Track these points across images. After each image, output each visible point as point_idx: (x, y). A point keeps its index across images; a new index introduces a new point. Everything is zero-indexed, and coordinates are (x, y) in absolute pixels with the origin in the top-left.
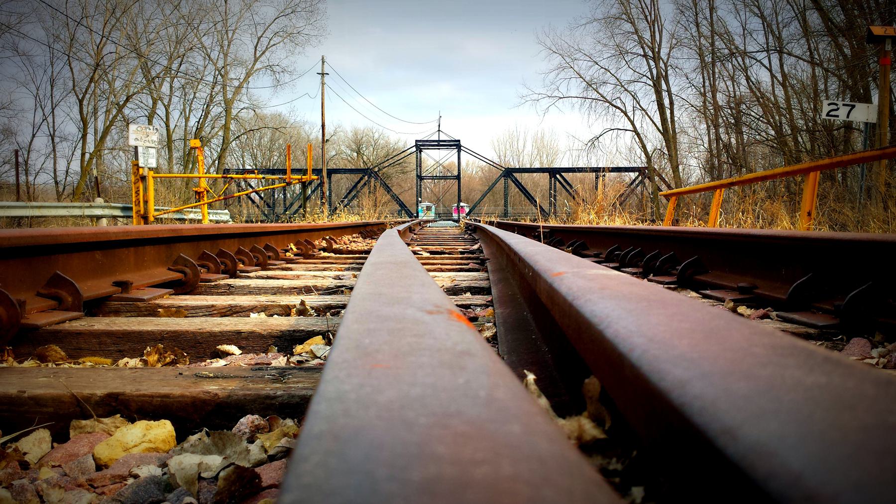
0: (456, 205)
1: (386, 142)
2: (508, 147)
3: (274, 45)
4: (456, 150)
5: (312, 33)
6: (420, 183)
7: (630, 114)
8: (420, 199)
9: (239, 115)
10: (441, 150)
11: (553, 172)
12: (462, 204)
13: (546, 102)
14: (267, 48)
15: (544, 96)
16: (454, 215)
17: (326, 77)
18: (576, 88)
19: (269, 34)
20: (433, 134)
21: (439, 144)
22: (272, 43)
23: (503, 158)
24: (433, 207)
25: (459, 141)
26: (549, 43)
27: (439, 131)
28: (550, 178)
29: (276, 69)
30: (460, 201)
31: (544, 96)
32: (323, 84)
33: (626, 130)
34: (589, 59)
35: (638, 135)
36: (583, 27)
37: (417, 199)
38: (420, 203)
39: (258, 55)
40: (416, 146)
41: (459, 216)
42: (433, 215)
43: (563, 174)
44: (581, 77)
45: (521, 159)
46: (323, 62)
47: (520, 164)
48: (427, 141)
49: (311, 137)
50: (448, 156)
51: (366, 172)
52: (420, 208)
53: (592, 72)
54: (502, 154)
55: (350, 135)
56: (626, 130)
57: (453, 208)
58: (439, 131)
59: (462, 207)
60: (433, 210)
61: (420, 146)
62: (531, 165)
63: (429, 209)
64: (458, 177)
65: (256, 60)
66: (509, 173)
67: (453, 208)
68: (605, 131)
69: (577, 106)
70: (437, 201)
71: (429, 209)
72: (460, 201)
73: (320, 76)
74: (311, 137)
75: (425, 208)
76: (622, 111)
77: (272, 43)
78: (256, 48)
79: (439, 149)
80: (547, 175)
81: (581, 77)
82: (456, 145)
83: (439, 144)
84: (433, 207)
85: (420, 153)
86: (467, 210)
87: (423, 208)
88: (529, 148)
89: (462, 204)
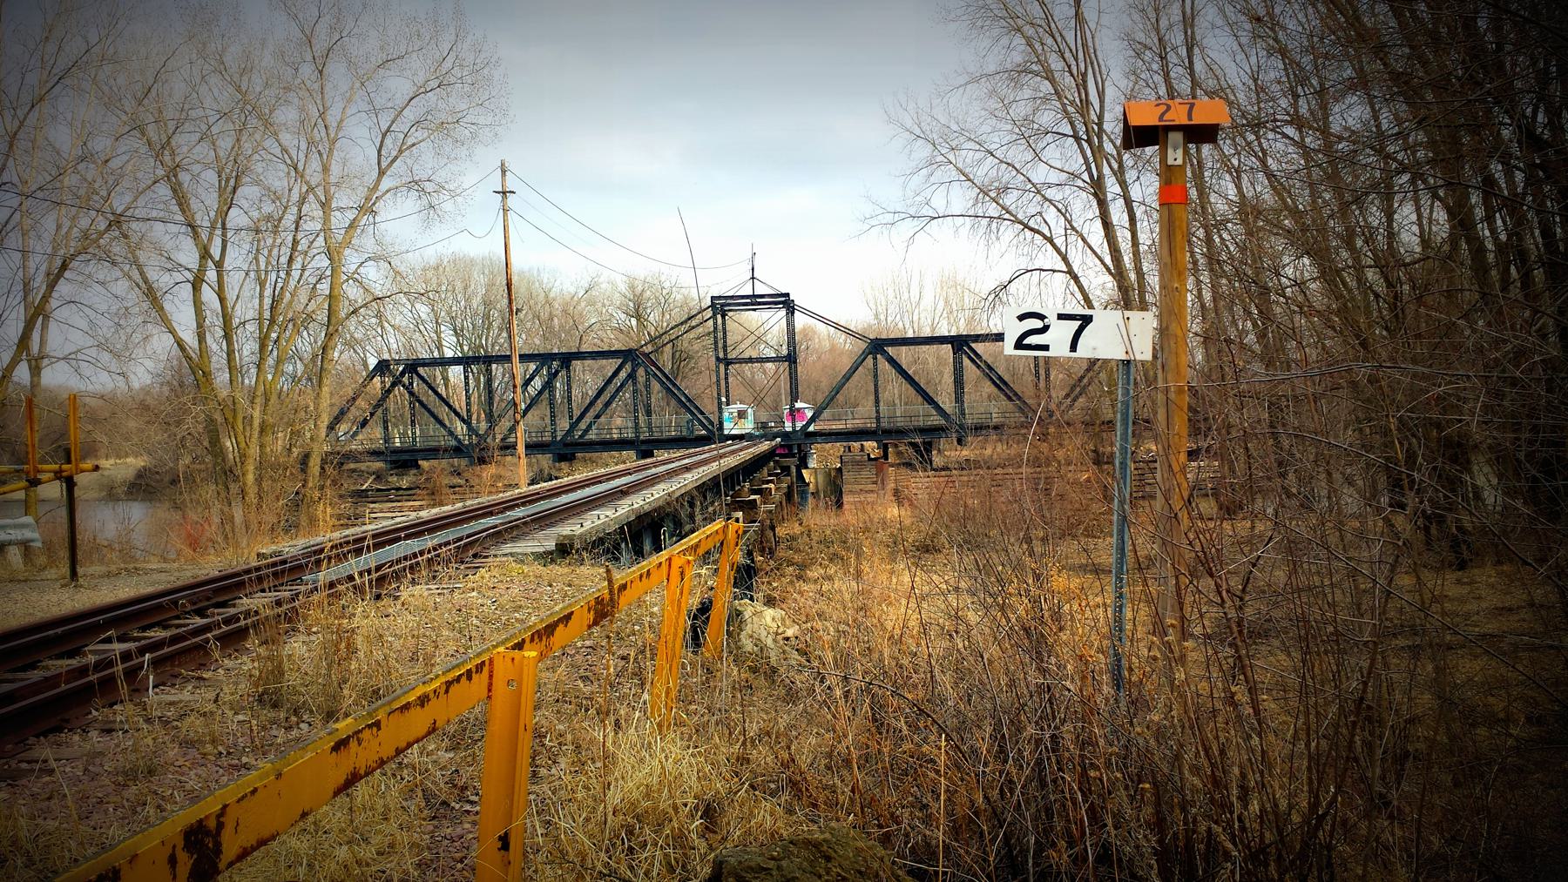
1: (686, 298)
2: (891, 297)
3: (414, 145)
4: (783, 312)
5: (481, 120)
6: (726, 369)
7: (1059, 242)
8: (724, 399)
9: (362, 270)
10: (757, 313)
11: (960, 343)
12: (798, 405)
13: (909, 226)
14: (401, 151)
15: (903, 216)
17: (510, 198)
18: (961, 198)
19: (401, 126)
20: (745, 282)
21: (754, 301)
22: (410, 141)
23: (882, 317)
24: (749, 410)
25: (788, 295)
26: (909, 123)
27: (753, 278)
29: (429, 187)
30: (794, 397)
31: (903, 216)
32: (505, 211)
33: (1054, 271)
34: (978, 147)
35: (1076, 278)
36: (961, 89)
37: (719, 399)
38: (728, 405)
39: (384, 165)
40: (713, 306)
41: (794, 426)
42: (751, 425)
43: (973, 345)
44: (969, 180)
45: (916, 318)
46: (504, 172)
47: (916, 326)
48: (732, 297)
49: (552, 295)
50: (772, 322)
51: (628, 355)
52: (726, 415)
53: (985, 170)
54: (880, 310)
55: (623, 288)
56: (1054, 271)
57: (785, 412)
58: (753, 278)
59: (799, 410)
61: (721, 306)
62: (933, 330)
63: (742, 414)
64: (791, 359)
65: (382, 173)
66: (878, 346)
67: (785, 412)
68: (1018, 274)
69: (964, 231)
70: (758, 401)
71: (742, 414)
72: (794, 397)
73: (499, 197)
74: (552, 295)
75: (736, 414)
76: (1045, 237)
77: (410, 141)
78: (379, 151)
79: (754, 310)
81: (969, 180)
82: (785, 302)
83: (754, 301)
85: (723, 317)
86: (809, 414)
87: (732, 413)
88: (927, 301)
89: (798, 405)
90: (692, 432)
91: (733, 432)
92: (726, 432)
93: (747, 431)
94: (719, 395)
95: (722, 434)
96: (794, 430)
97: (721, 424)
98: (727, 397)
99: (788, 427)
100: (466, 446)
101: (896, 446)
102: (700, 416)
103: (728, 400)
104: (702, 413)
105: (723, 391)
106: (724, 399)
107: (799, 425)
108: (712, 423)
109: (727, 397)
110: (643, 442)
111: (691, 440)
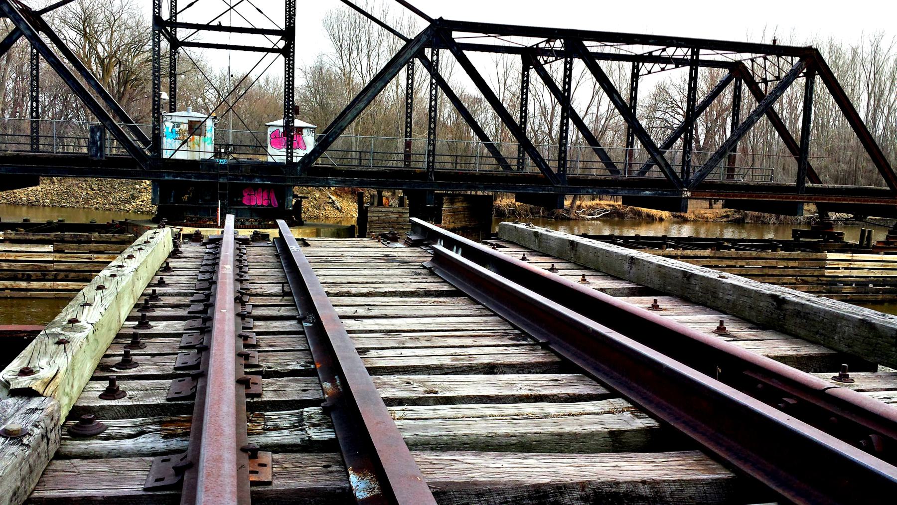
0: (281, 122)
8: (165, 96)
12: (298, 123)
16: (270, 150)
24: (209, 123)
28: (526, 68)
37: (156, 94)
38: (173, 109)
41: (290, 155)
42: (210, 148)
52: (168, 126)
59: (300, 129)
60: (210, 135)
63: (195, 128)
71: (195, 128)
75: (185, 127)
80: (518, 57)
84: (209, 123)
87: (178, 125)
90: (101, 149)
91: (180, 156)
92: (166, 155)
93: (203, 156)
96: (290, 163)
97: (157, 139)
99: (277, 155)
101: (452, 201)
103: (173, 96)
104: (125, 119)
106: (165, 96)
107: (299, 154)
109: (173, 96)
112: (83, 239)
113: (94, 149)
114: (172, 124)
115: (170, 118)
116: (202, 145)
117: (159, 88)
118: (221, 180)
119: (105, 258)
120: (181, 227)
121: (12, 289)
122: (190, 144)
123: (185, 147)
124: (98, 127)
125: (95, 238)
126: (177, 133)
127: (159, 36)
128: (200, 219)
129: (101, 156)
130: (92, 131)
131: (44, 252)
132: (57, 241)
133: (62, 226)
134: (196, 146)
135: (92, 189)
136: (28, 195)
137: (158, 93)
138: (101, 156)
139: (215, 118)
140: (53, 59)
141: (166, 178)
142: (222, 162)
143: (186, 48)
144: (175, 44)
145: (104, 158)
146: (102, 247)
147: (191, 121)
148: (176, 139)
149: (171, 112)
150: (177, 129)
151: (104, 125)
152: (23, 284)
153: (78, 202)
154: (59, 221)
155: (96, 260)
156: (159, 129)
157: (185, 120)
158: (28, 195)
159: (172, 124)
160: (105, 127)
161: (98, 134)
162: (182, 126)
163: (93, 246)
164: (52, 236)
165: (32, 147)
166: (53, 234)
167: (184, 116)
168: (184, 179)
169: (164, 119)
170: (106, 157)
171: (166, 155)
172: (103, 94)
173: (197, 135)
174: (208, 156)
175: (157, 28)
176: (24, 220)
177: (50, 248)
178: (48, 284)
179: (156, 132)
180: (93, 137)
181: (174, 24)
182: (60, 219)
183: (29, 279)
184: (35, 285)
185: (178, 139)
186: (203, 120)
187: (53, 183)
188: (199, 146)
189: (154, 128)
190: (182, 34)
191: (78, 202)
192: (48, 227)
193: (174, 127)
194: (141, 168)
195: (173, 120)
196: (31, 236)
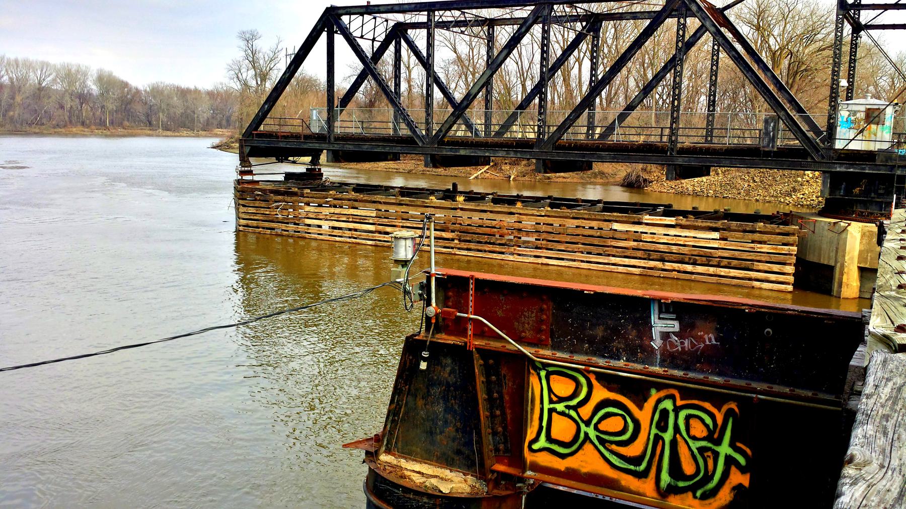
8: (844, 83)
24: (890, 111)
52: (843, 114)
63: (873, 116)
71: (873, 116)
75: (862, 115)
84: (890, 111)
90: (773, 140)
92: (839, 145)
94: (835, 74)
95: (831, 148)
98: (851, 77)
100: (421, 138)
102: (792, 113)
103: (851, 83)
104: (800, 110)
105: (844, 68)
106: (844, 83)
108: (817, 132)
109: (851, 83)
110: (684, 151)
111: (767, 154)
112: (748, 229)
113: (767, 139)
114: (848, 113)
115: (846, 106)
116: (879, 134)
117: (838, 76)
118: (899, 172)
119: (768, 248)
120: (849, 222)
121: (679, 271)
122: (865, 133)
123: (859, 137)
124: (772, 118)
125: (760, 228)
126: (852, 122)
127: (843, 21)
128: (872, 214)
129: (773, 147)
130: (766, 122)
131: (709, 238)
132: (724, 230)
133: (729, 216)
134: (873, 136)
135: (754, 181)
136: (694, 185)
137: (837, 80)
138: (773, 147)
139: (897, 104)
140: (734, 53)
141: (838, 169)
142: (901, 152)
143: (872, 32)
144: (858, 28)
145: (775, 149)
146: (765, 237)
147: (869, 109)
148: (850, 128)
149: (847, 100)
150: (853, 118)
151: (778, 115)
152: (689, 268)
153: (739, 193)
154: (725, 210)
155: (759, 250)
156: (834, 118)
157: (863, 108)
158: (694, 185)
159: (848, 113)
160: (779, 117)
161: (772, 125)
162: (858, 115)
163: (757, 236)
164: (719, 224)
165: (706, 139)
166: (720, 222)
167: (860, 104)
168: (857, 171)
169: (840, 108)
170: (778, 148)
171: (839, 145)
172: (778, 85)
173: (874, 124)
174: (885, 146)
175: (842, 12)
176: (694, 208)
177: (716, 235)
178: (712, 270)
179: (832, 121)
180: (766, 128)
181: (859, 7)
182: (726, 208)
183: (695, 263)
184: (700, 269)
185: (853, 128)
186: (884, 107)
187: (718, 174)
188: (875, 135)
189: (830, 118)
190: (865, 17)
191: (739, 193)
192: (714, 216)
193: (849, 116)
194: (813, 158)
195: (850, 108)
196: (699, 223)
